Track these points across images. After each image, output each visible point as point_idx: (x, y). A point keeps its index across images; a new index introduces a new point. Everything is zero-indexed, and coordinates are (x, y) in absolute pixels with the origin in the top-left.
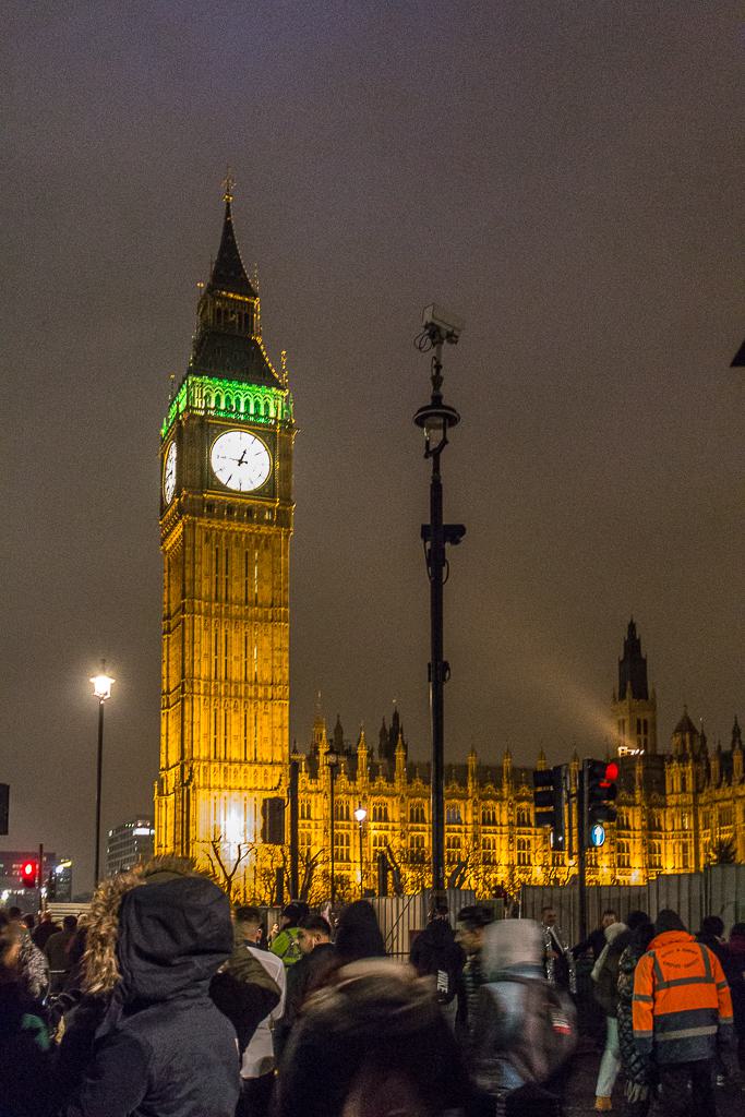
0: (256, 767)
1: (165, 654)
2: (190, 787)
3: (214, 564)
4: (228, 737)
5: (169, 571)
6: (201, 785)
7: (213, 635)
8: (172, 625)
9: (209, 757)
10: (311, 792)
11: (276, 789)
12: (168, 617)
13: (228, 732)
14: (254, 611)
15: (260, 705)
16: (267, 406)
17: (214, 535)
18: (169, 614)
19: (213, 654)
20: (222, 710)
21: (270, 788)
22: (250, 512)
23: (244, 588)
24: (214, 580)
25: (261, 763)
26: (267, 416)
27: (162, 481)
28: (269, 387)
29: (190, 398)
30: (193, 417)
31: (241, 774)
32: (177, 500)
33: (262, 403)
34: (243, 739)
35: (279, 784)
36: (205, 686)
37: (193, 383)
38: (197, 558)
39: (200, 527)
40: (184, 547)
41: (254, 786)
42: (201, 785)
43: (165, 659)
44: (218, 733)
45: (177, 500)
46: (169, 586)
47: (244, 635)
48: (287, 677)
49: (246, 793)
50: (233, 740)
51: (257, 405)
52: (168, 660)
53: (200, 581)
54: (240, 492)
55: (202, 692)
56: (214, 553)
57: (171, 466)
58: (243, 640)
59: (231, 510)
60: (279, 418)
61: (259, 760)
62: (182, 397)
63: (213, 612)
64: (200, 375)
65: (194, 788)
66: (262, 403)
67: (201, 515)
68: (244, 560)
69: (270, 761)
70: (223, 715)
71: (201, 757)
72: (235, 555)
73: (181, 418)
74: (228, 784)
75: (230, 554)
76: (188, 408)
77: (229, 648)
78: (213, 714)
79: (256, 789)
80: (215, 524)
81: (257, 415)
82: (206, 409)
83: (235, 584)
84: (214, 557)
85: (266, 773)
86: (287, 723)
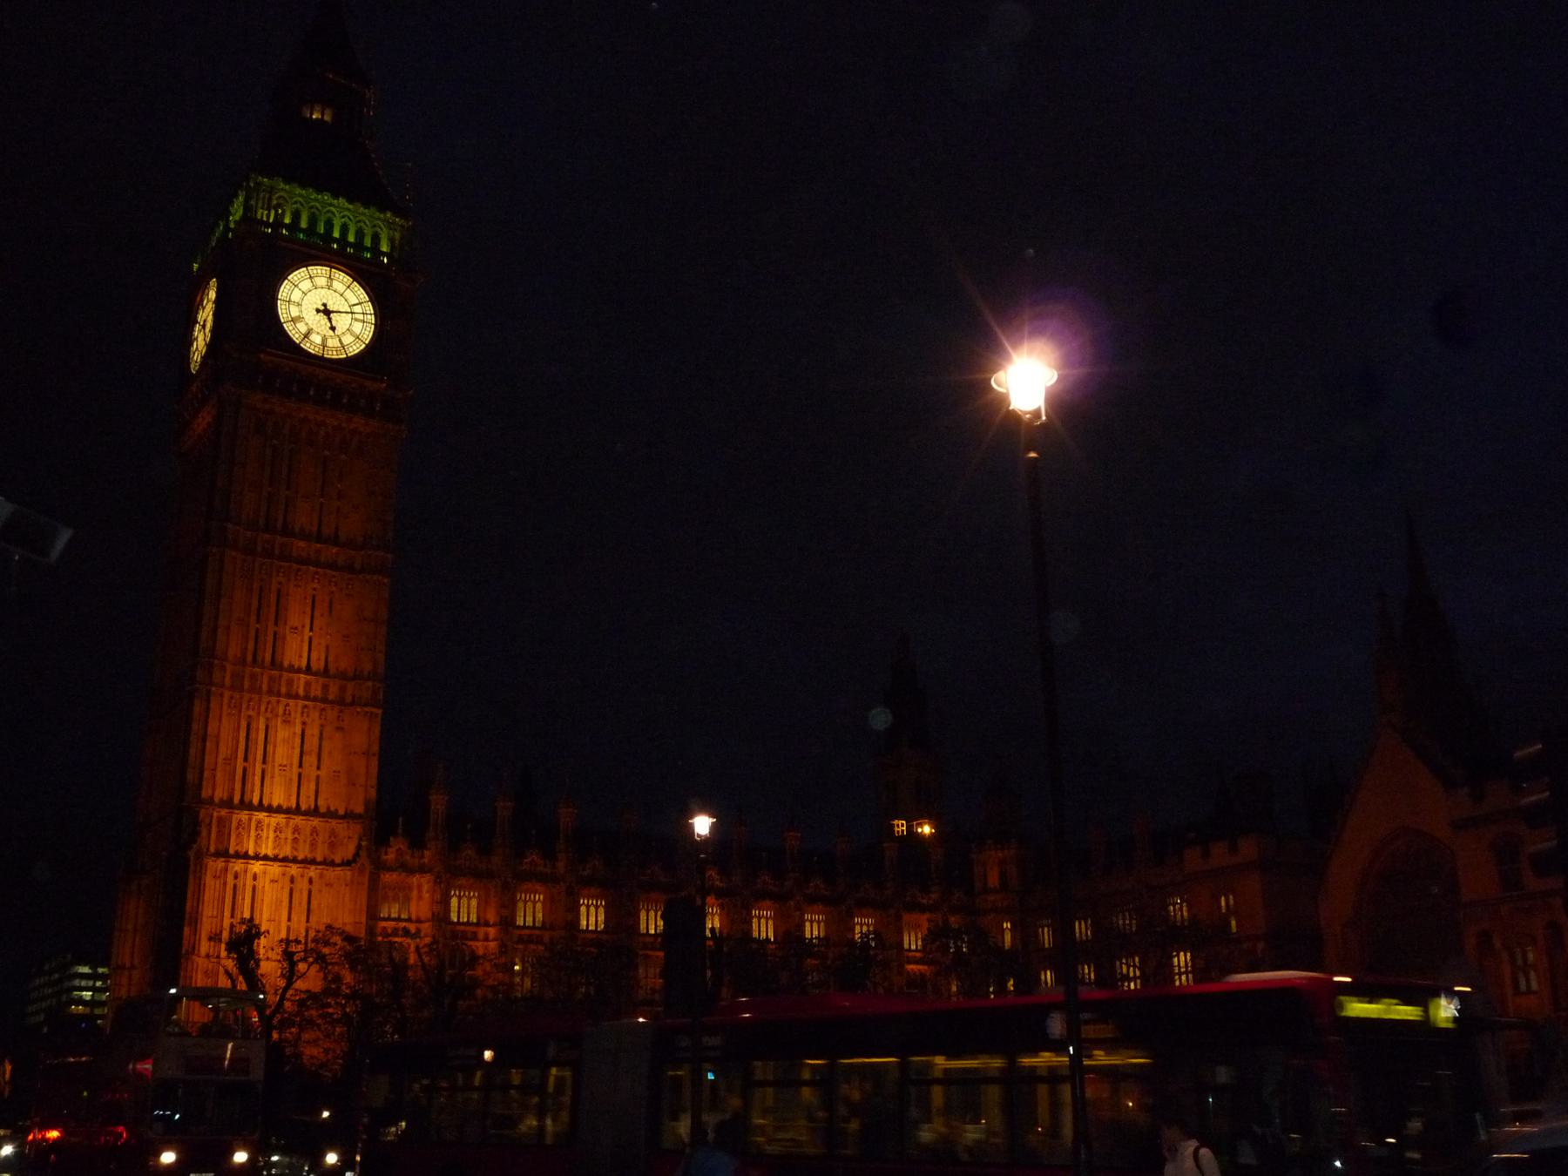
0: (316, 822)
2: (191, 854)
4: (269, 768)
6: (212, 849)
9: (231, 799)
10: (411, 871)
13: (269, 758)
21: (338, 861)
25: (323, 815)
28: (382, 210)
29: (247, 208)
33: (368, 232)
34: (295, 769)
35: (356, 855)
41: (310, 856)
42: (212, 849)
44: (251, 757)
49: (294, 870)
50: (277, 770)
58: (309, 601)
61: (323, 810)
62: (237, 212)
63: (259, 549)
65: (200, 856)
66: (368, 232)
69: (341, 812)
71: (217, 800)
74: (263, 852)
78: (244, 724)
79: (313, 862)
81: (358, 245)
85: (333, 833)
86: (376, 748)
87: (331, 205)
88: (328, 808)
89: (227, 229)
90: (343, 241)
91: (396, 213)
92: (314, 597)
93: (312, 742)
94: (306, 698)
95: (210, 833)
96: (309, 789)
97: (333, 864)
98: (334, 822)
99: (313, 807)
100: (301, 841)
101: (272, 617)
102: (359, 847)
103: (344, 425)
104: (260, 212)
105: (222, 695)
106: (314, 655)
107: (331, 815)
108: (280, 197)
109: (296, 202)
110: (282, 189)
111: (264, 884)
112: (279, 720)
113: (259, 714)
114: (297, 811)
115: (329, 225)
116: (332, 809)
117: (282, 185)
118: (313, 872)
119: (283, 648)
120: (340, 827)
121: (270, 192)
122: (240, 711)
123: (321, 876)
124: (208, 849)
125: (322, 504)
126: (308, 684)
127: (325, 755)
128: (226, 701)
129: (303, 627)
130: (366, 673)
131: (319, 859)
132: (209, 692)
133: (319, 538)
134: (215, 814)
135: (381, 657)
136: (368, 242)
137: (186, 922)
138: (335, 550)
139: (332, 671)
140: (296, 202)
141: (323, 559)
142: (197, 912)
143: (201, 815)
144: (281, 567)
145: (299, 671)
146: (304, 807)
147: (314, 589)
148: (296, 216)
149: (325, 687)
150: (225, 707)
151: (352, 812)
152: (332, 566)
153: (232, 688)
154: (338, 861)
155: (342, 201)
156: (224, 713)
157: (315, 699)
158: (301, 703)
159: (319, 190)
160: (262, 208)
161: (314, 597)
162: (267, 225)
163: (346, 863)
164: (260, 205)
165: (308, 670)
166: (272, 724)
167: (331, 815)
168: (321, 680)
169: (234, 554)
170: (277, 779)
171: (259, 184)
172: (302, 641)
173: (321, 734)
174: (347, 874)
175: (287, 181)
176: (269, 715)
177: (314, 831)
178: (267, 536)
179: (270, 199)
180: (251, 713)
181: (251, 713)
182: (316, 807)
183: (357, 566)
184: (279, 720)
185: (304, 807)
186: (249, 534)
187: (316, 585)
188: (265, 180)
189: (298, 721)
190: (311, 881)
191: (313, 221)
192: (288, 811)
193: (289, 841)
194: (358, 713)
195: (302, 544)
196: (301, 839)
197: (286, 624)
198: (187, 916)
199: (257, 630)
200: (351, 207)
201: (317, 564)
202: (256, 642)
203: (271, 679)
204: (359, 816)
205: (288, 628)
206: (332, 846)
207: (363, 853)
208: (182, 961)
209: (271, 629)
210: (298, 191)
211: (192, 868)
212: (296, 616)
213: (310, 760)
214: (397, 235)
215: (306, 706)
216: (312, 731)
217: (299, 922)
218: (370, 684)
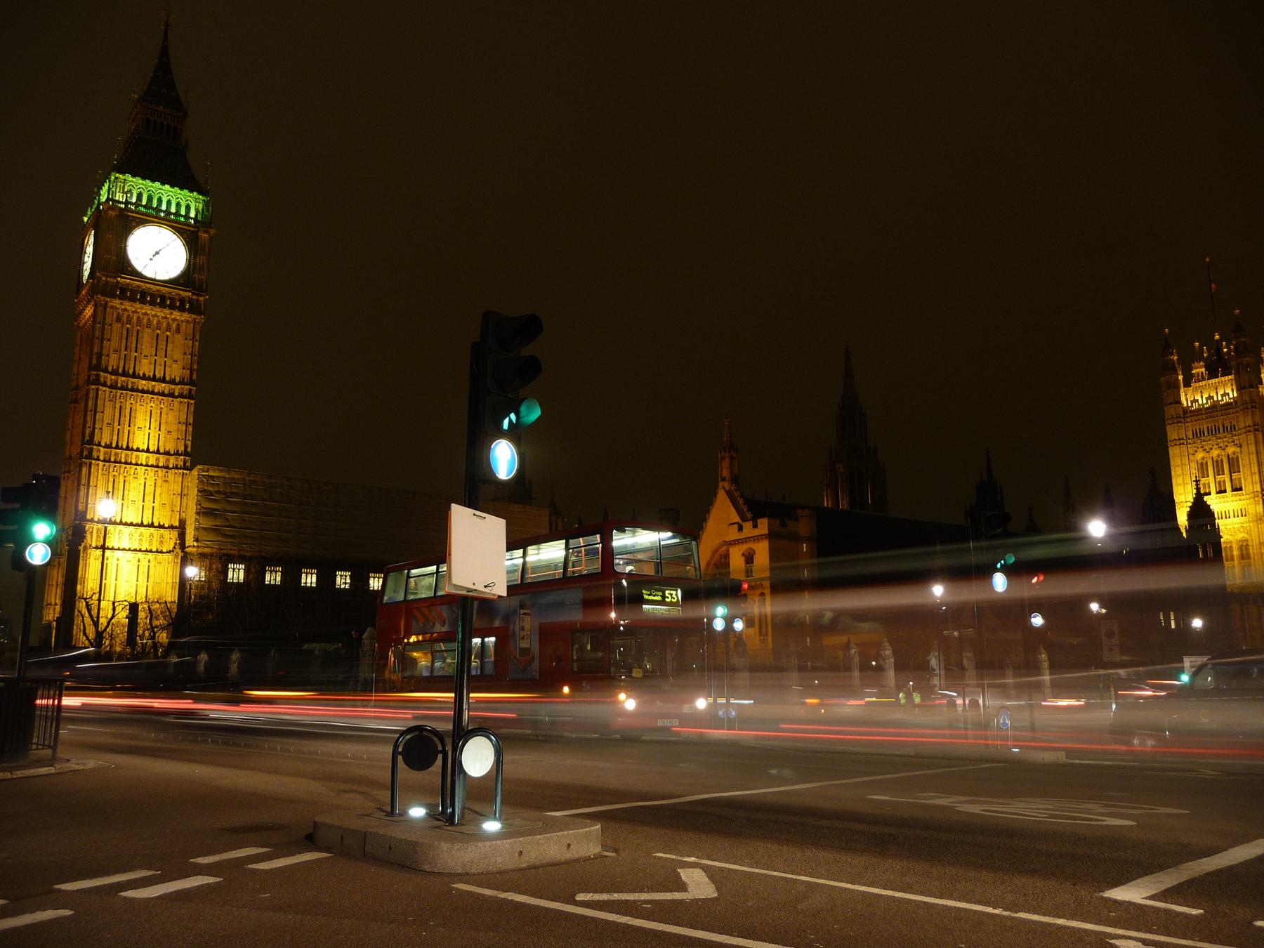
0: (152, 530)
1: (70, 421)
2: (81, 548)
3: (124, 341)
4: (125, 502)
5: (81, 345)
7: (118, 406)
8: (79, 396)
11: (169, 552)
12: (77, 388)
14: (160, 387)
15: (161, 472)
16: (188, 208)
17: (125, 316)
18: (77, 385)
19: (116, 423)
20: (121, 477)
22: (163, 298)
23: (153, 366)
24: (123, 356)
25: (156, 527)
26: (187, 216)
27: (81, 263)
30: (113, 208)
31: (136, 536)
32: (91, 281)
34: (141, 503)
35: (174, 548)
36: (105, 453)
37: (116, 178)
38: (107, 335)
39: (112, 307)
40: (94, 322)
41: (149, 549)
43: (70, 426)
45: (91, 281)
46: (80, 359)
47: (149, 408)
48: (189, 449)
51: (178, 205)
52: (73, 427)
53: (108, 356)
54: (155, 280)
55: (101, 458)
56: (125, 332)
57: (90, 249)
58: (149, 413)
59: (144, 294)
60: (199, 218)
61: (156, 524)
64: (124, 173)
65: (85, 548)
67: (114, 296)
68: (155, 341)
69: (166, 525)
70: (122, 481)
72: (146, 335)
73: (101, 207)
75: (140, 334)
76: (108, 199)
77: (132, 419)
78: (111, 479)
80: (127, 305)
81: (177, 214)
82: (127, 203)
83: (145, 361)
84: (125, 335)
85: (162, 536)
87: (160, 189)
88: (159, 523)
89: (99, 204)
90: (168, 212)
91: (200, 193)
92: (151, 411)
93: (150, 489)
94: (147, 465)
95: (92, 536)
96: (148, 513)
97: (161, 552)
98: (162, 531)
99: (150, 523)
100: (144, 541)
101: (127, 423)
102: (176, 544)
103: (168, 316)
104: (118, 194)
105: (98, 465)
106: (151, 443)
107: (161, 526)
108: (130, 185)
109: (139, 188)
110: (131, 181)
111: (123, 563)
112: (132, 477)
113: (119, 474)
114: (142, 525)
115: (160, 200)
116: (162, 524)
117: (131, 179)
118: (150, 556)
119: (133, 439)
120: (166, 533)
121: (124, 183)
122: (109, 473)
123: (155, 558)
124: (90, 546)
125: (155, 360)
126: (148, 458)
127: (157, 495)
128: (101, 467)
129: (145, 427)
130: (180, 452)
131: (154, 550)
132: (91, 463)
133: (154, 379)
134: (95, 527)
135: (189, 443)
136: (183, 212)
137: (79, 583)
138: (163, 385)
139: (162, 451)
140: (139, 188)
141: (156, 391)
142: (85, 578)
143: (87, 528)
144: (132, 395)
145: (143, 451)
146: (145, 523)
147: (151, 407)
148: (140, 196)
149: (157, 459)
150: (100, 471)
151: (172, 525)
152: (162, 394)
153: (104, 461)
154: (164, 550)
155: (167, 187)
156: (100, 474)
157: (152, 466)
158: (144, 468)
159: (153, 181)
160: (119, 192)
161: (151, 411)
162: (122, 203)
163: (169, 552)
164: (118, 190)
165: (148, 451)
166: (127, 479)
167: (161, 526)
168: (155, 455)
169: (104, 388)
170: (130, 508)
171: (116, 178)
172: (144, 435)
173: (155, 483)
174: (170, 557)
175: (133, 176)
176: (126, 474)
177: (151, 535)
178: (123, 378)
179: (124, 187)
180: (115, 473)
181: (115, 473)
182: (152, 523)
183: (176, 394)
184: (132, 477)
185: (145, 523)
186: (113, 377)
187: (152, 404)
188: (121, 176)
189: (143, 477)
190: (149, 562)
191: (150, 199)
192: (137, 525)
193: (138, 540)
194: (176, 473)
195: (144, 382)
196: (144, 539)
197: (135, 425)
198: (79, 579)
199: (119, 430)
200: (172, 190)
201: (153, 393)
202: (118, 436)
203: (126, 455)
204: (176, 527)
205: (136, 428)
206: (161, 542)
207: (177, 547)
208: (77, 602)
209: (127, 428)
210: (141, 181)
211: (81, 555)
212: (141, 419)
213: (149, 498)
214: (201, 206)
215: (147, 470)
216: (150, 483)
217: (143, 582)
218: (182, 457)
